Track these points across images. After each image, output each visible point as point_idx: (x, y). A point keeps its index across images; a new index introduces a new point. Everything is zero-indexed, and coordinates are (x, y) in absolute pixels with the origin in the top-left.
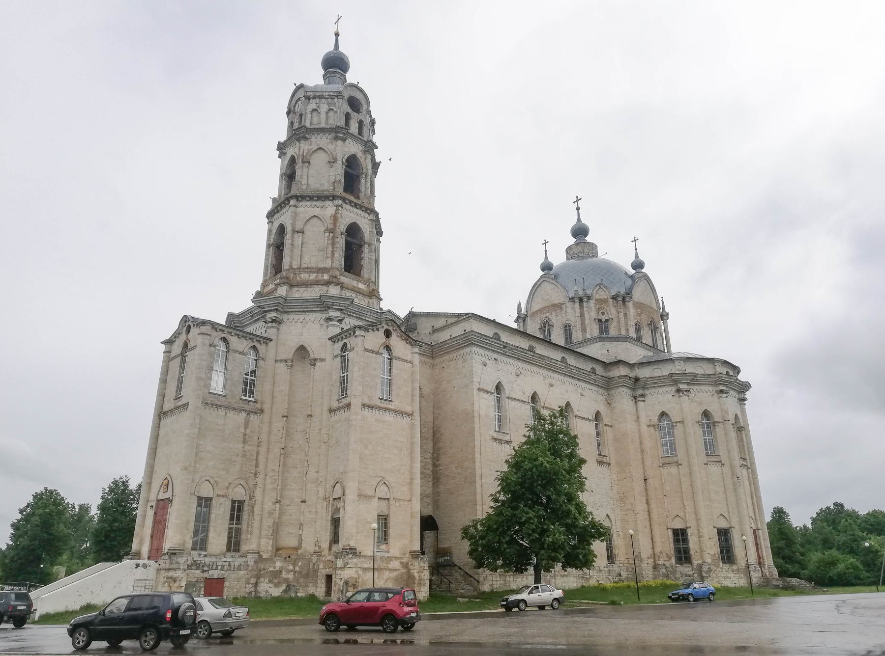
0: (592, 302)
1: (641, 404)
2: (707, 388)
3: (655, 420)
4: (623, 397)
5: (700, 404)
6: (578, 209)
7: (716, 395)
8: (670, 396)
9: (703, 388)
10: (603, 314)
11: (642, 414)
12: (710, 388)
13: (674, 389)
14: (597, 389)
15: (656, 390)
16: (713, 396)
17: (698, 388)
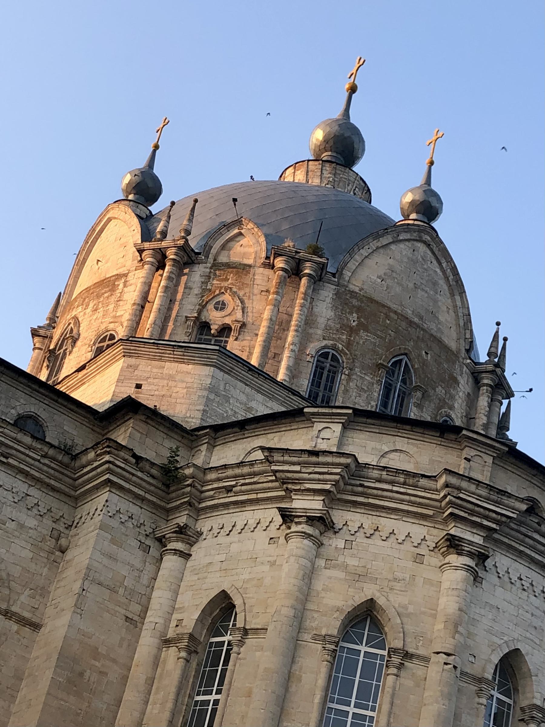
0: (198, 273)
1: (170, 562)
2: (404, 527)
3: (189, 615)
4: (102, 523)
5: (359, 577)
6: (353, 89)
7: (435, 560)
8: (261, 537)
9: (387, 523)
10: (221, 306)
11: (160, 597)
12: (417, 530)
13: (271, 514)
14: (21, 486)
15: (226, 519)
16: (419, 559)
17: (368, 521)
